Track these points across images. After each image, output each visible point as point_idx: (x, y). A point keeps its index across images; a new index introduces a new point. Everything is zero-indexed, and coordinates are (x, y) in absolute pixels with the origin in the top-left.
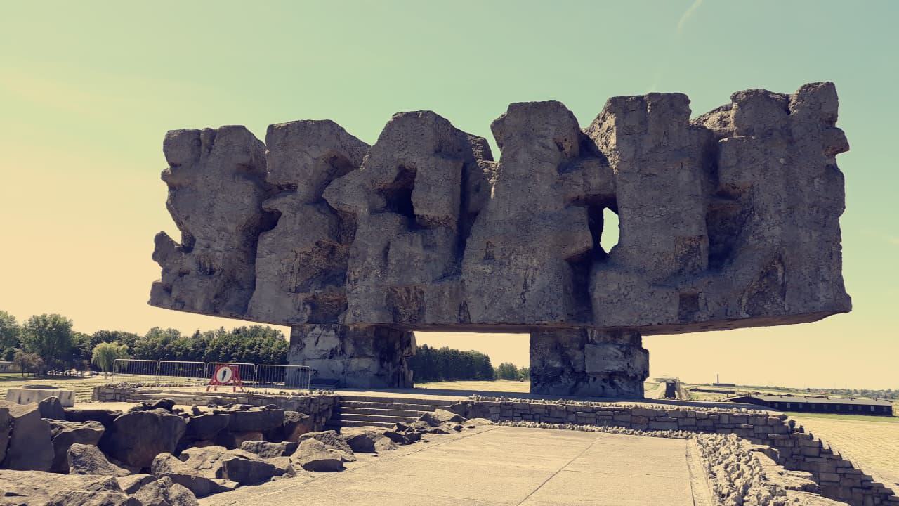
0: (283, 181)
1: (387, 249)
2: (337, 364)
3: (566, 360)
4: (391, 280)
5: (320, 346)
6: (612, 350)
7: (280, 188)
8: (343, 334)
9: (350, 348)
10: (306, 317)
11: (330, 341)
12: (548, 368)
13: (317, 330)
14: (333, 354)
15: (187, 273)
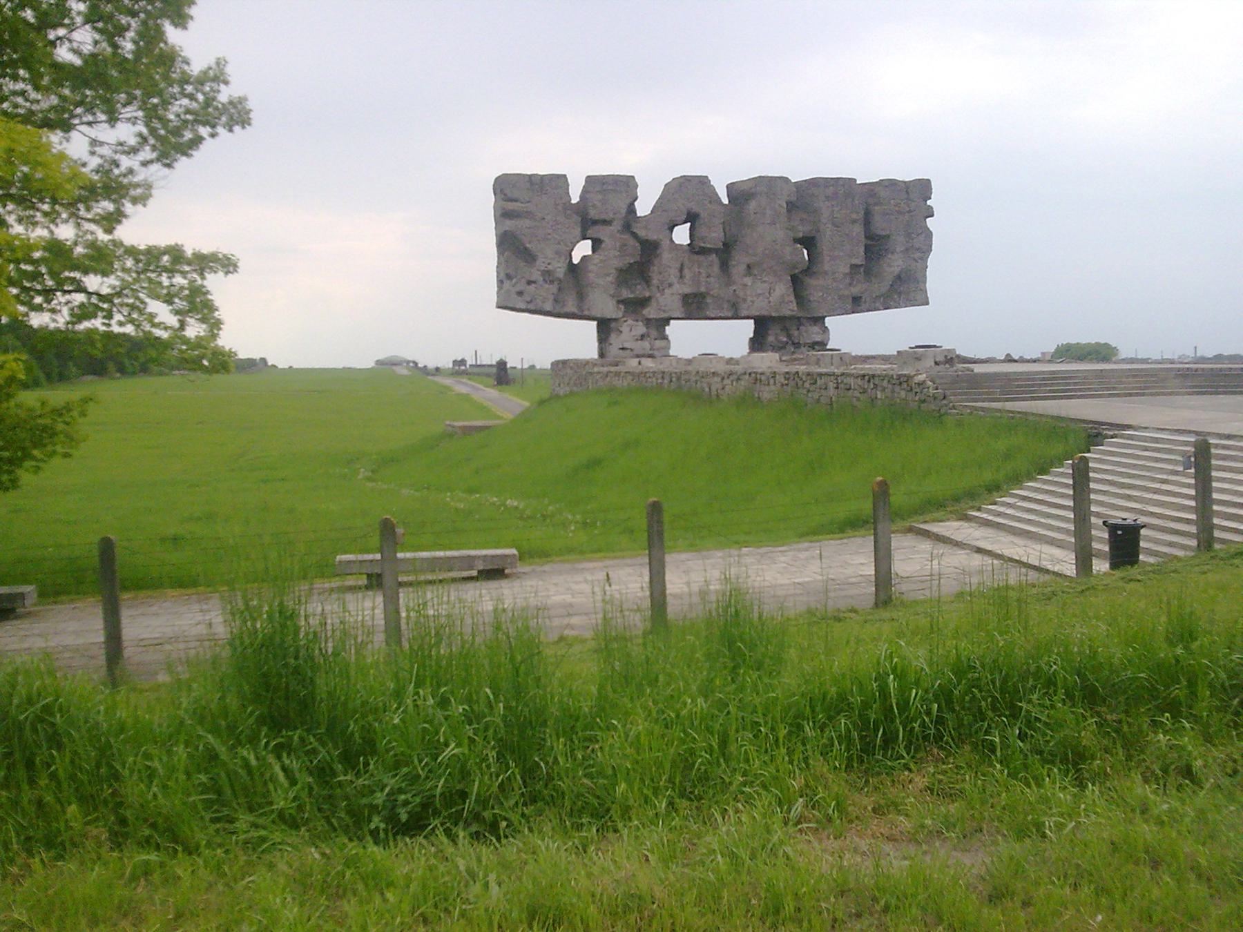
0: (603, 217)
1: (681, 270)
2: (646, 344)
3: (789, 336)
4: (687, 290)
5: (633, 333)
6: (816, 329)
7: (595, 222)
8: (648, 322)
9: (654, 333)
10: (620, 315)
11: (641, 329)
12: (780, 342)
13: (630, 322)
14: (642, 337)
15: (534, 282)
